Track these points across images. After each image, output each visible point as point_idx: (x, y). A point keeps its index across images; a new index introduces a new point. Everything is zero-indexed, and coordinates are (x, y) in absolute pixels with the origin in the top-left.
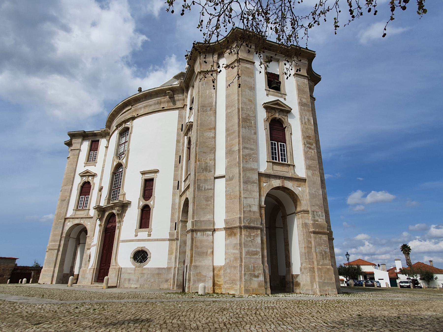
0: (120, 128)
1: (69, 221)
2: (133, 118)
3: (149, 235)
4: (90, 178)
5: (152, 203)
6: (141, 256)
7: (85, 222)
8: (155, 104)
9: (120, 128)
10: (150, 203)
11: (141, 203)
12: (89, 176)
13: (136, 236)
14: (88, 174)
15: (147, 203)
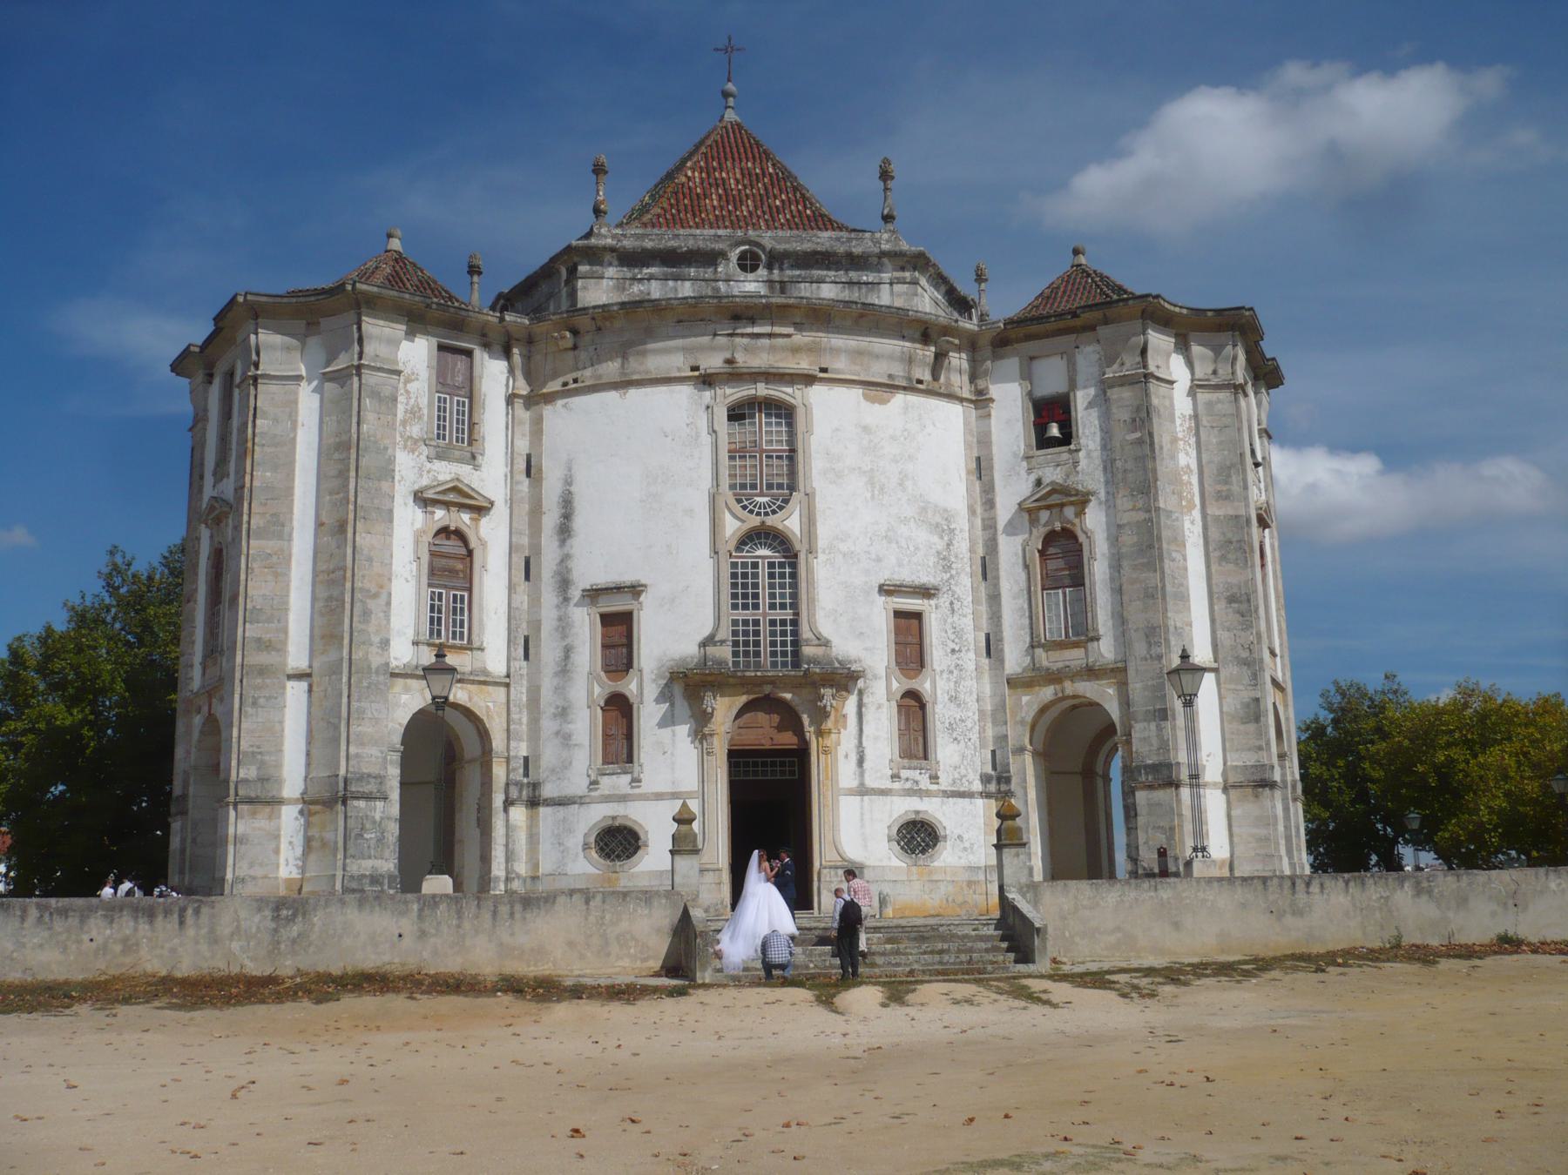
0: (735, 393)
1: (407, 690)
2: (809, 380)
3: (934, 778)
4: (466, 517)
5: (927, 685)
6: (918, 836)
7: (475, 699)
8: (891, 357)
9: (735, 393)
10: (925, 686)
11: (895, 685)
12: (462, 506)
13: (895, 777)
14: (451, 497)
15: (913, 684)
